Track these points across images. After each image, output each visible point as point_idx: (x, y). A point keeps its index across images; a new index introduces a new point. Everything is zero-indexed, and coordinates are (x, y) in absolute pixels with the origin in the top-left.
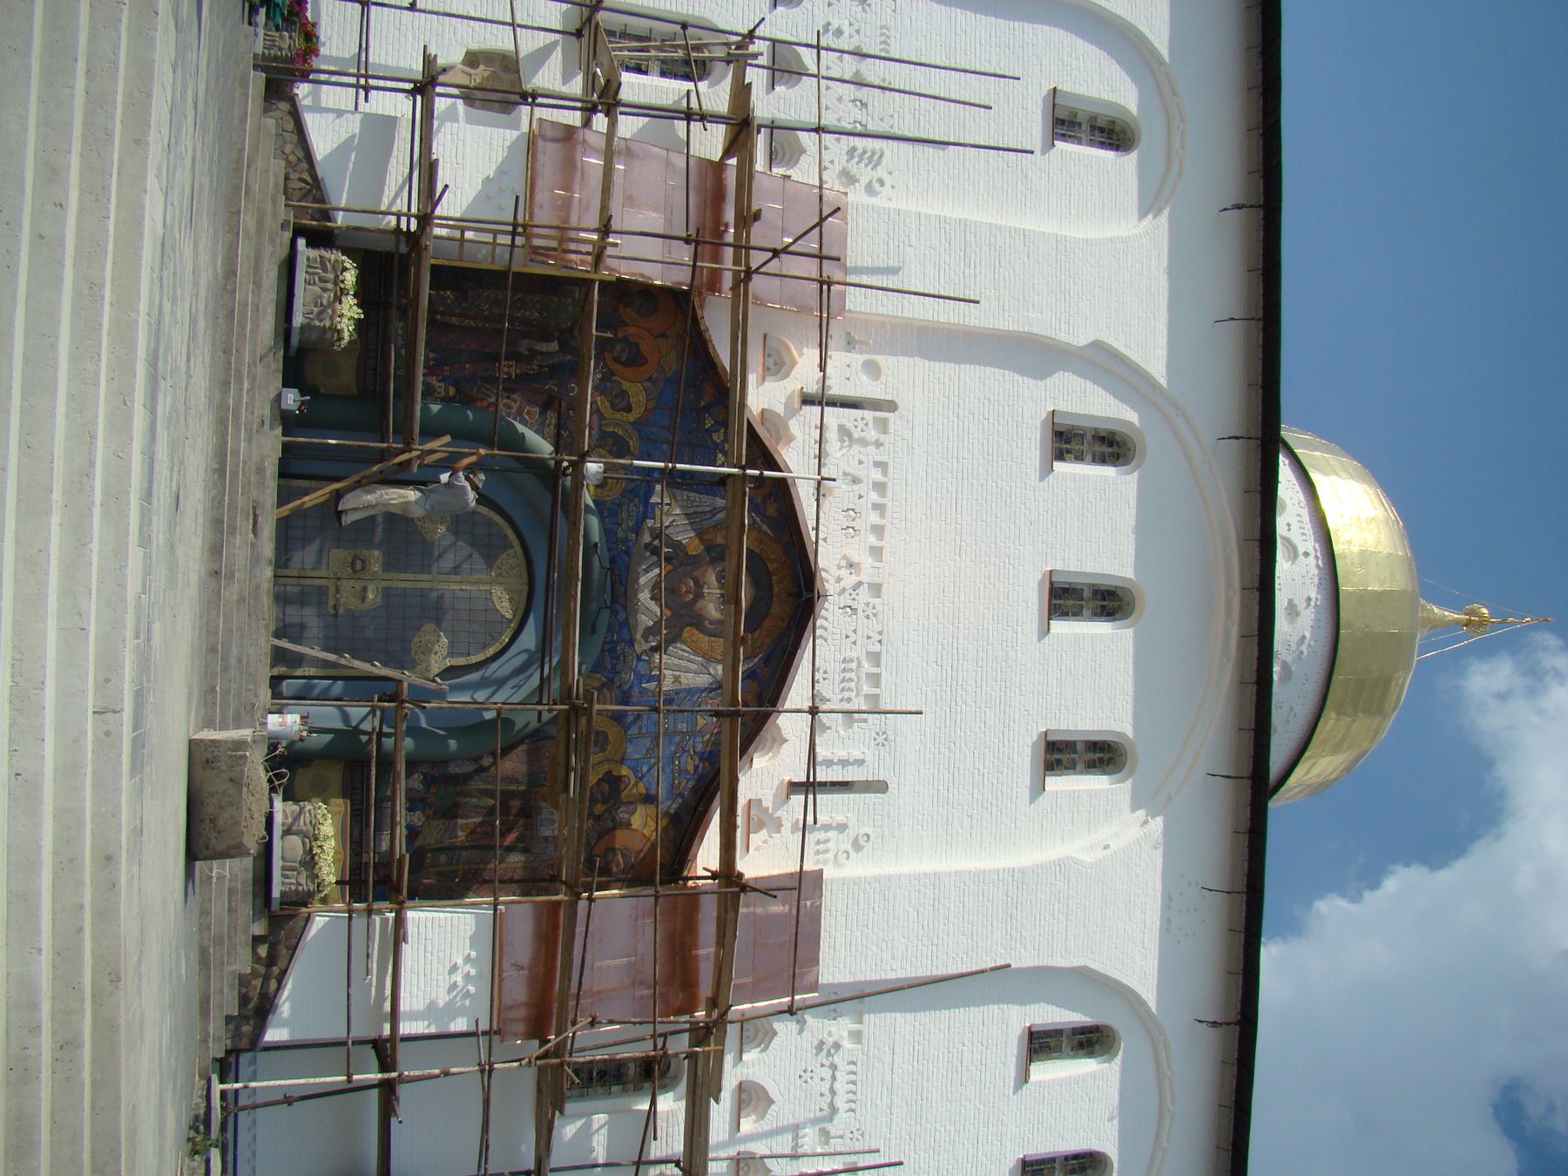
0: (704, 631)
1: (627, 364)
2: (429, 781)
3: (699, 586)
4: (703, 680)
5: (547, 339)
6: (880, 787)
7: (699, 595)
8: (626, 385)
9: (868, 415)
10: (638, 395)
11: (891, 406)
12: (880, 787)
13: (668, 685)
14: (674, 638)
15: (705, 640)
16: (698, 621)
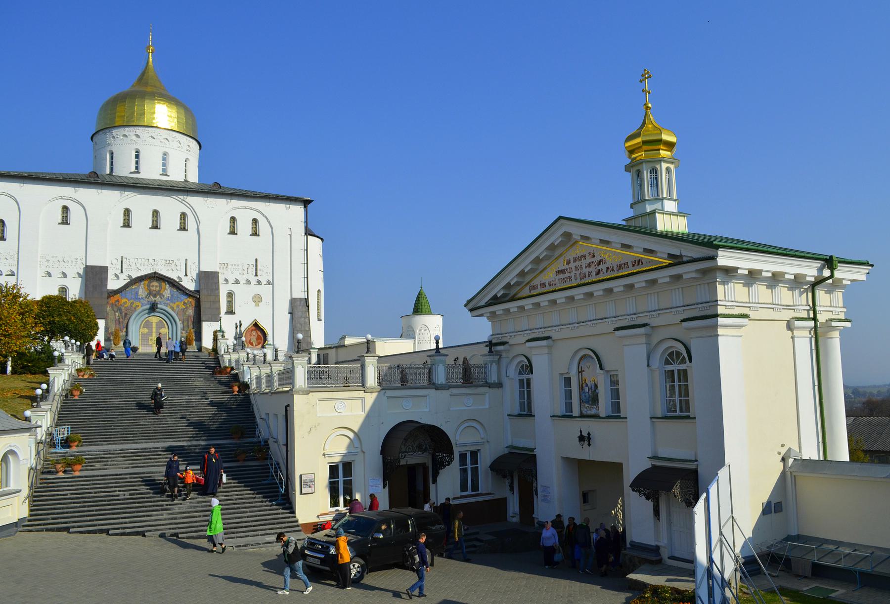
0: (161, 290)
1: (119, 302)
2: (184, 330)
3: (153, 291)
4: (169, 290)
5: (115, 315)
6: (186, 260)
7: (155, 291)
8: (122, 302)
9: (124, 260)
10: (124, 300)
11: (122, 257)
12: (186, 260)
13: (170, 296)
14: (162, 294)
15: (162, 290)
16: (159, 291)
